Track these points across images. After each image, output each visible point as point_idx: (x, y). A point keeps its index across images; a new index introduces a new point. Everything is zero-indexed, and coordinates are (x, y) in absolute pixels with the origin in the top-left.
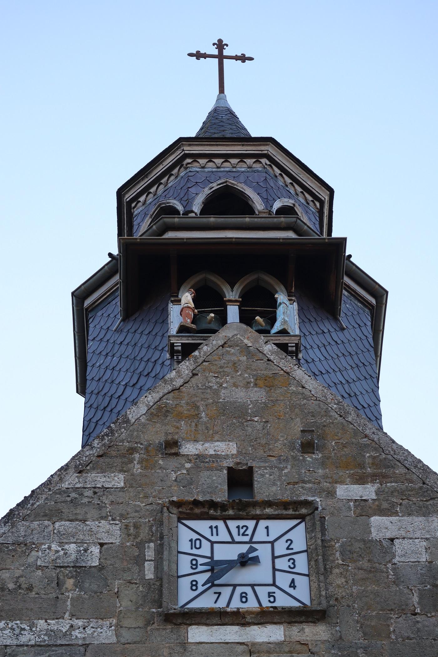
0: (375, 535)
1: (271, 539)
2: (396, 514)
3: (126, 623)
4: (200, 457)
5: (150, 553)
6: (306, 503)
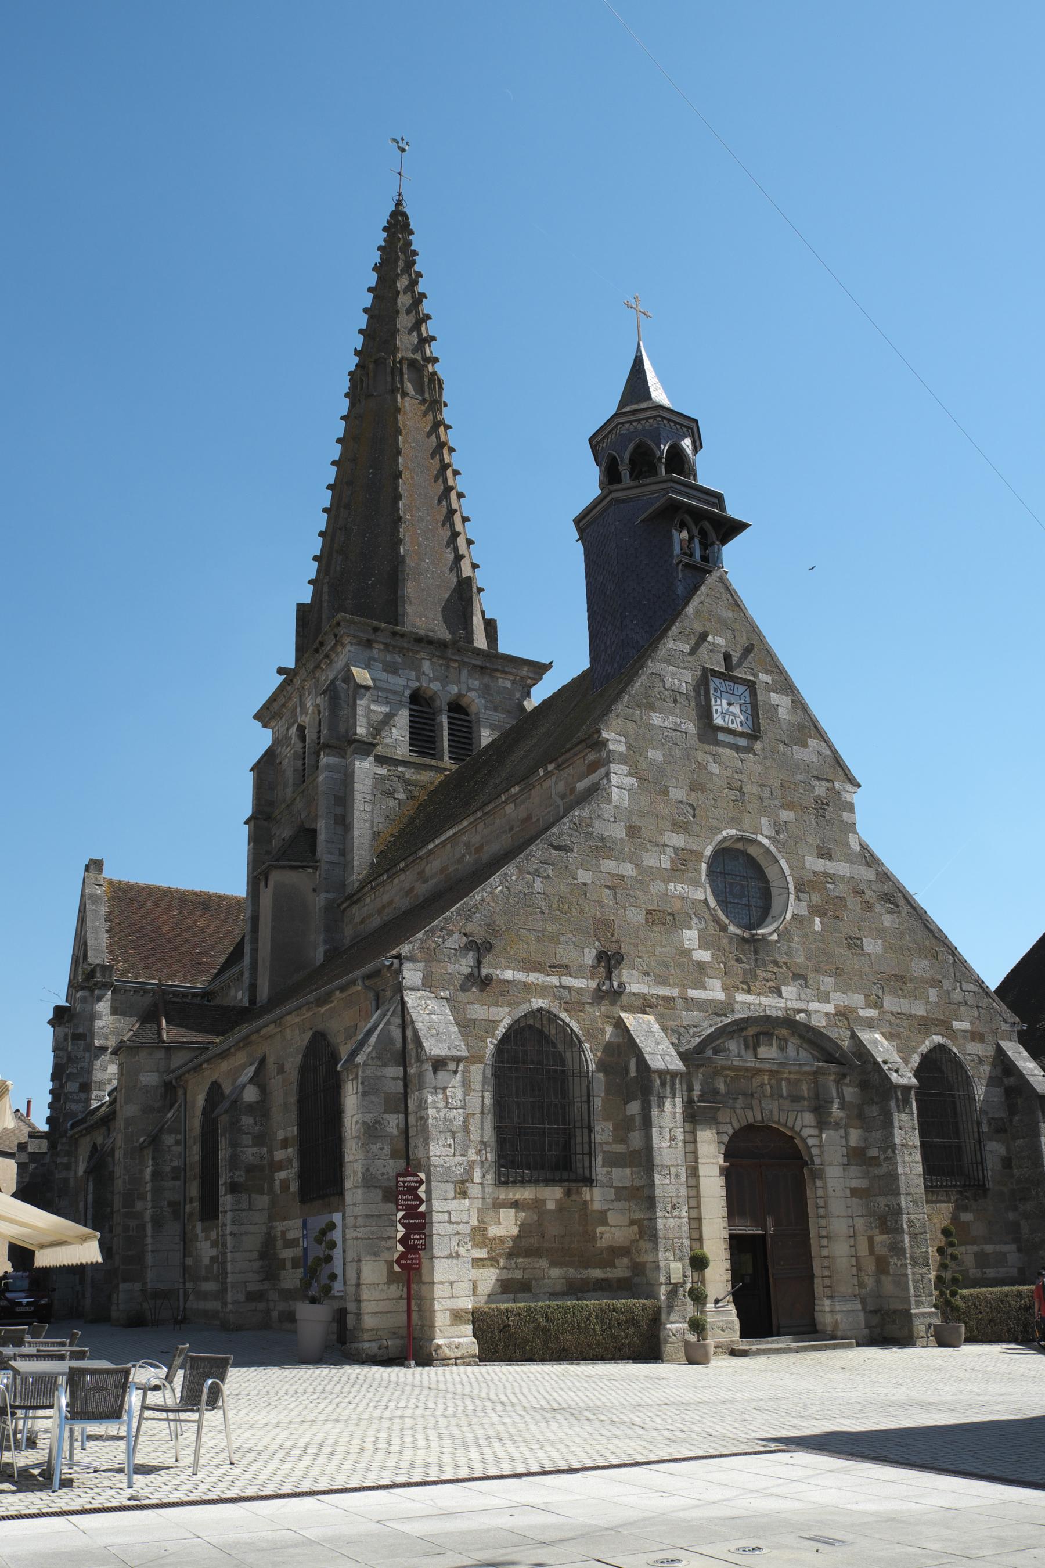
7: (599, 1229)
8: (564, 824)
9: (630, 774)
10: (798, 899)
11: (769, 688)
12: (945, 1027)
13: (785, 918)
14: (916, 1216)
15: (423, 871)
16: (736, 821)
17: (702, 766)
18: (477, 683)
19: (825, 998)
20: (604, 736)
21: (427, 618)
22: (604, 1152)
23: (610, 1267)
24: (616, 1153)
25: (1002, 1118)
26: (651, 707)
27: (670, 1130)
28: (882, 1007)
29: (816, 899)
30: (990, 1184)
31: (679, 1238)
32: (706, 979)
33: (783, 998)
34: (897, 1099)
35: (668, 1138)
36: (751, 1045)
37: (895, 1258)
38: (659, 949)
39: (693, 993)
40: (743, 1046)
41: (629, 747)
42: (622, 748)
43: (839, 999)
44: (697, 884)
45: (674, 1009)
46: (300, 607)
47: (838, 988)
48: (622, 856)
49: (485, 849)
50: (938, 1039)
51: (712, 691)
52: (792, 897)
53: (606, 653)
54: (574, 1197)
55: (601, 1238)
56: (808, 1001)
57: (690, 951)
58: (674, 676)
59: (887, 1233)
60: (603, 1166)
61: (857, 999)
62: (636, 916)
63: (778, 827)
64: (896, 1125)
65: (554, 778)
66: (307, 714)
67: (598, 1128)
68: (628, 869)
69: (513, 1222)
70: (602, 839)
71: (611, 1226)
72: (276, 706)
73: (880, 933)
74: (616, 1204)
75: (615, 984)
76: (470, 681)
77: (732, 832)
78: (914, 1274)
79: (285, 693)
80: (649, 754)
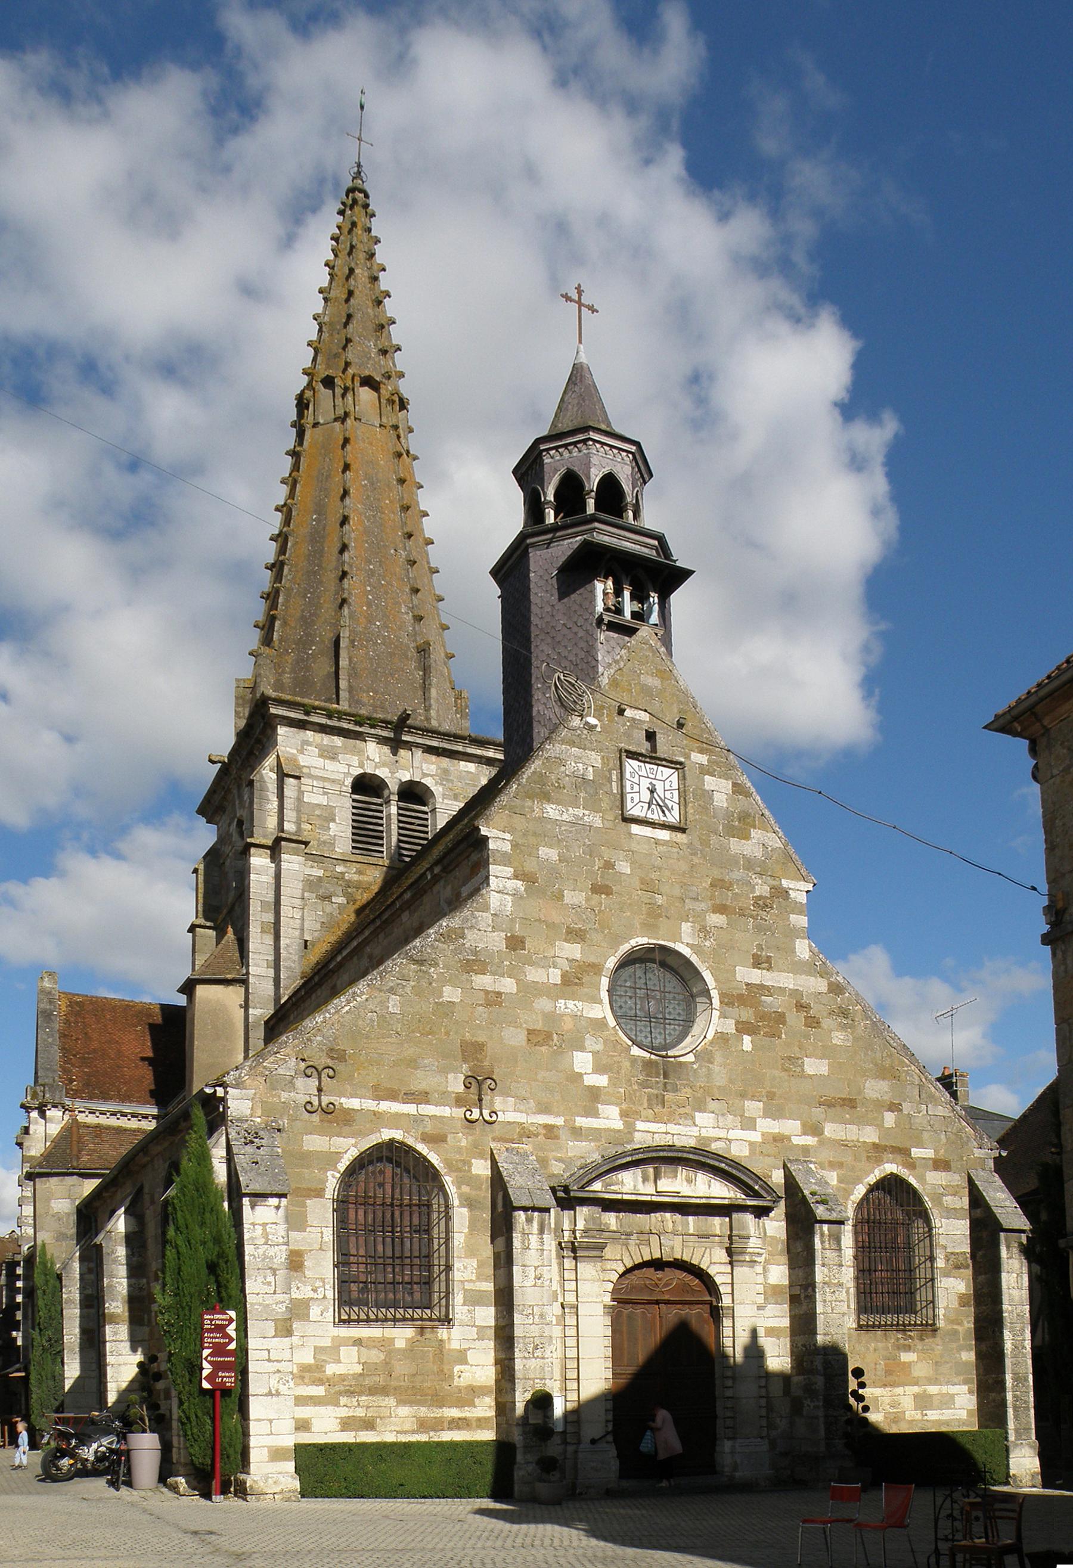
0: (707, 787)
1: (663, 779)
2: (715, 776)
3: (606, 817)
4: (633, 719)
5: (614, 777)
6: (681, 763)
7: (457, 1368)
8: (429, 936)
9: (516, 877)
10: (723, 1016)
11: (704, 770)
12: (903, 1152)
13: (705, 1037)
14: (835, 1357)
16: (649, 928)
17: (609, 865)
18: (433, 767)
19: (749, 1124)
20: (483, 833)
21: (376, 692)
22: (465, 1290)
23: (469, 1406)
24: (480, 1291)
25: (965, 1253)
26: (547, 797)
27: (536, 1268)
28: (822, 1133)
29: (747, 1014)
30: (941, 1323)
31: (541, 1379)
32: (599, 1105)
33: (697, 1126)
34: (822, 1235)
35: (533, 1276)
36: (652, 1177)
37: (809, 1400)
38: (542, 1074)
39: (581, 1121)
40: (640, 1180)
41: (515, 845)
42: (507, 847)
43: (768, 1126)
44: (596, 1000)
45: (557, 1137)
47: (768, 1114)
48: (500, 971)
50: (891, 1168)
51: (628, 775)
52: (716, 1014)
54: (428, 1336)
55: (459, 1377)
56: (728, 1130)
57: (580, 1075)
58: (578, 759)
59: (803, 1375)
60: (464, 1304)
61: (791, 1127)
62: (516, 1038)
63: (704, 931)
64: (818, 1261)
65: (442, 882)
66: (244, 807)
67: (457, 1265)
68: (508, 985)
69: (356, 1360)
70: (475, 953)
71: (472, 1365)
72: (217, 798)
73: (827, 1052)
74: (478, 1344)
75: (486, 1113)
76: (424, 766)
77: (644, 940)
78: (826, 1416)
79: (223, 784)
80: (540, 853)
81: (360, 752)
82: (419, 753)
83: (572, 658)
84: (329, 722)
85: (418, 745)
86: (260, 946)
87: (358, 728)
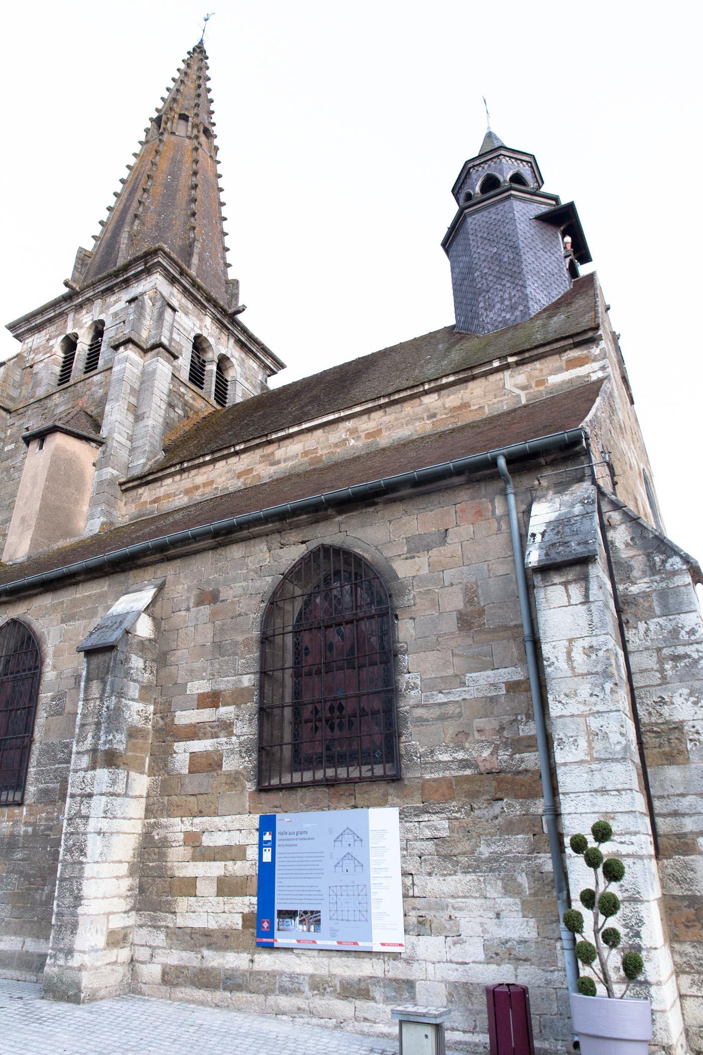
15: (272, 454)
46: (81, 250)
49: (385, 434)
53: (502, 303)
81: (201, 320)
82: (232, 341)
83: (548, 269)
84: (191, 289)
85: (233, 335)
86: (125, 420)
87: (205, 303)
